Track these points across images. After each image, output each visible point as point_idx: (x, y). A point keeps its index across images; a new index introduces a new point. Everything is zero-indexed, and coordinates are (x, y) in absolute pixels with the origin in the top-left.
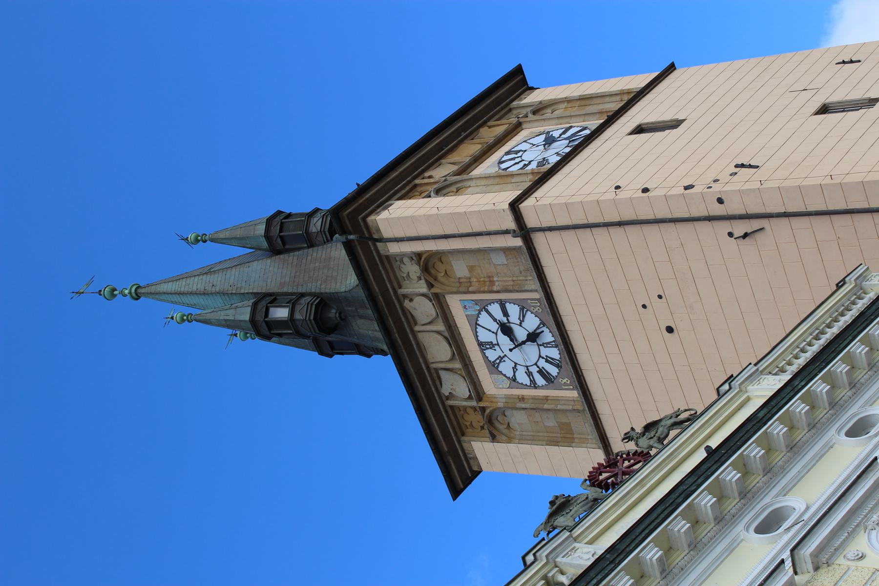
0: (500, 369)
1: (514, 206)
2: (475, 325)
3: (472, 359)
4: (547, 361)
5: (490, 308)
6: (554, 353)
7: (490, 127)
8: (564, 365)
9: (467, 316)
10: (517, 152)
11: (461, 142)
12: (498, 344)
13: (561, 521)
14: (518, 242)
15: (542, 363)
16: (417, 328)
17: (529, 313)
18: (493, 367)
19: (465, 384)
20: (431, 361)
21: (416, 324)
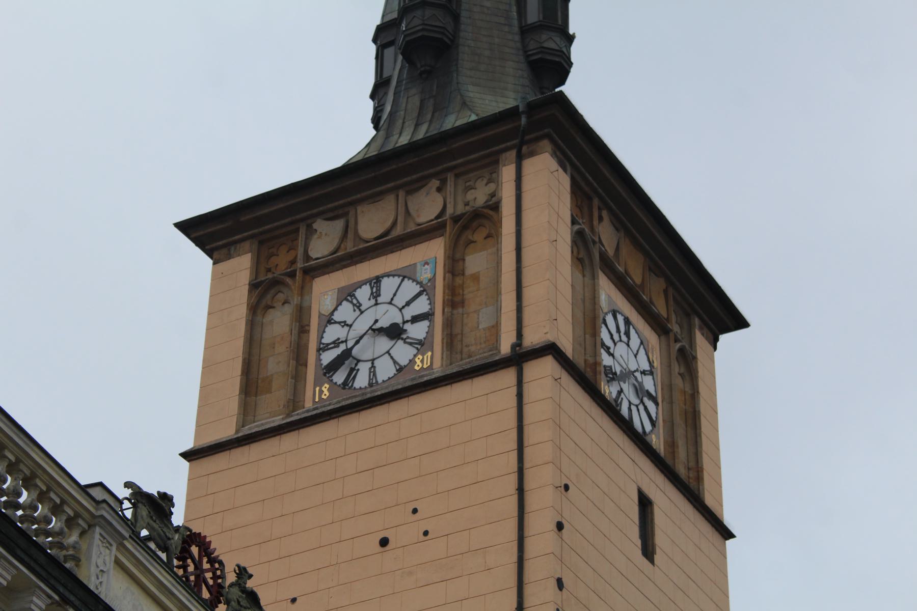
0: (345, 303)
1: (550, 349)
2: (406, 274)
3: (358, 266)
5: (424, 298)
6: (362, 381)
7: (666, 292)
8: (347, 393)
9: (415, 264)
10: (627, 334)
11: (646, 254)
12: (376, 304)
13: (144, 511)
14: (505, 348)
16: (402, 194)
17: (415, 351)
19: (326, 253)
20: (359, 209)
21: (409, 193)
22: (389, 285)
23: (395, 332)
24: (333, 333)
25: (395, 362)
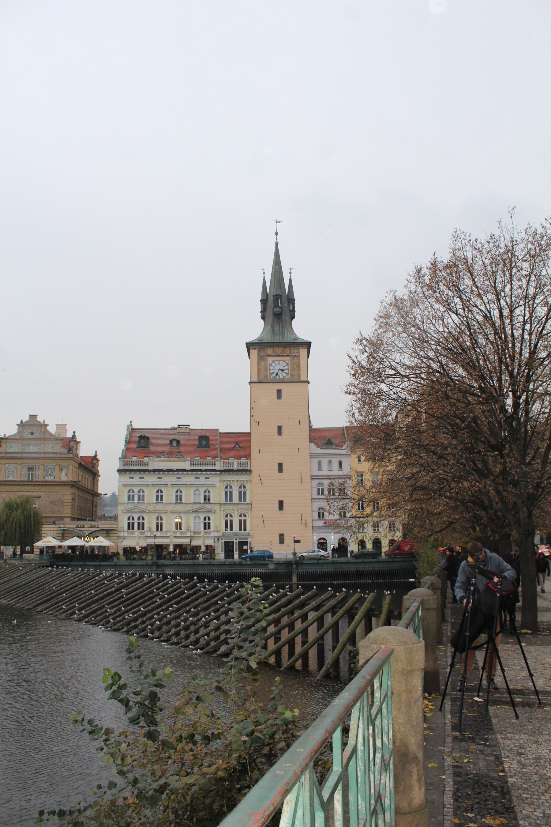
6: (277, 377)
22: (281, 362)
23: (282, 370)
24: (271, 367)
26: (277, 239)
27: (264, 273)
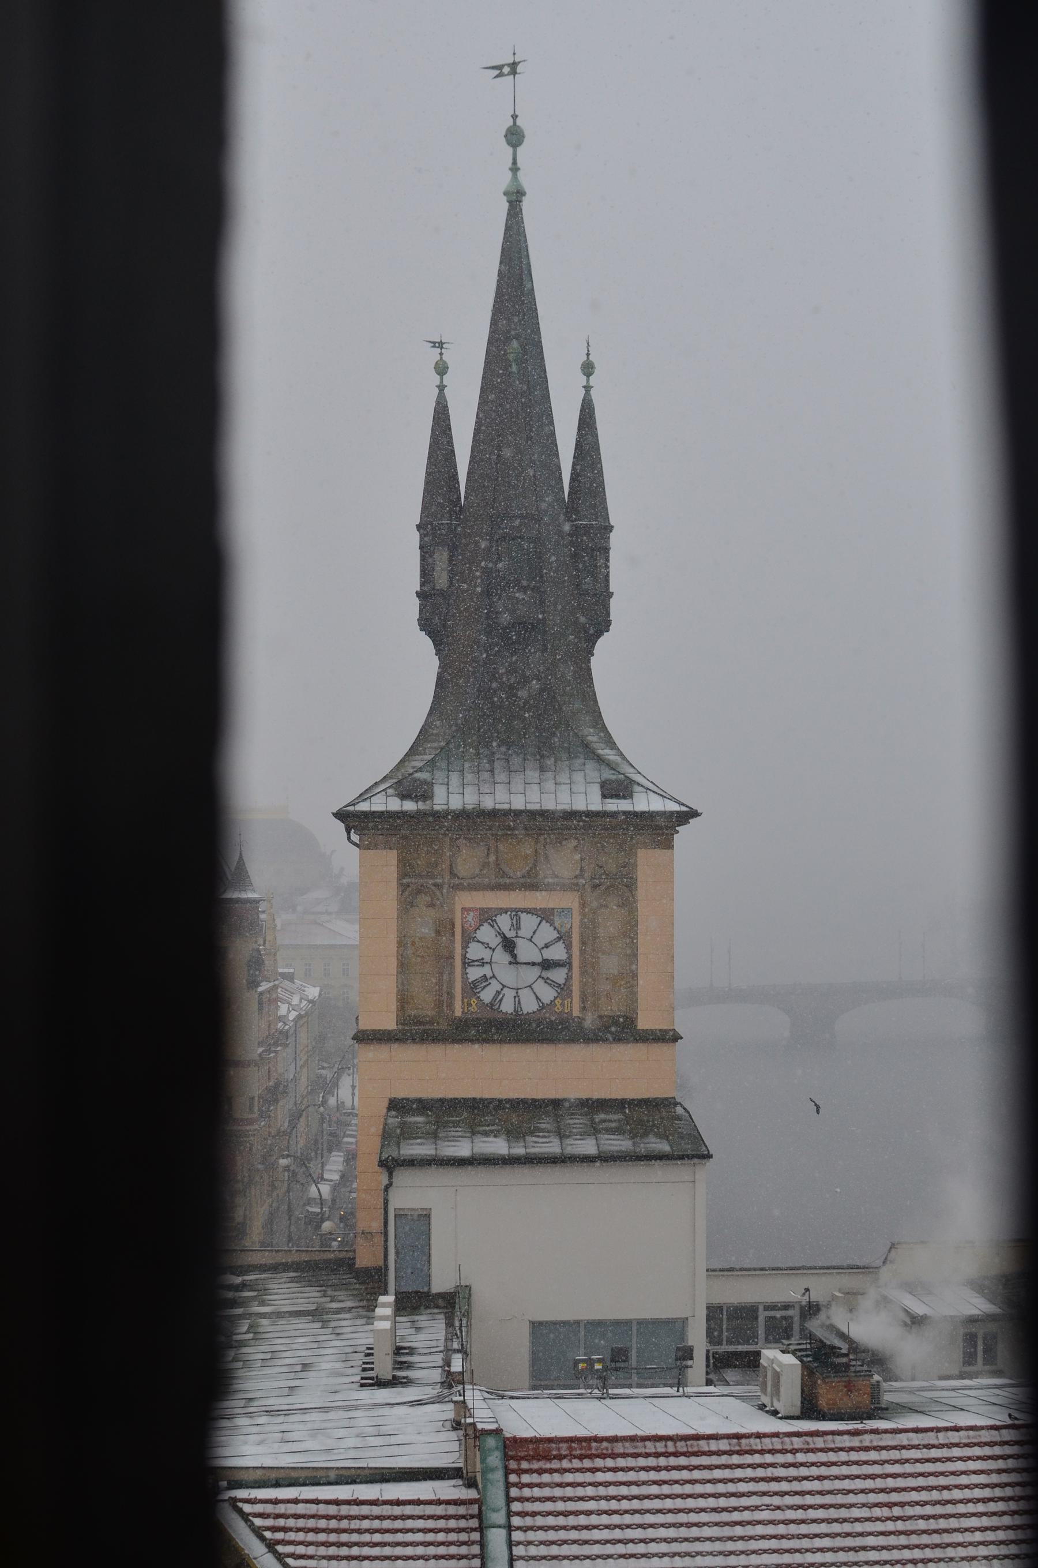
4: (498, 993)
5: (560, 945)
15: (495, 986)
17: (556, 995)
18: (487, 916)
22: (528, 922)
24: (475, 951)
25: (537, 998)
26: (515, 169)
27: (441, 369)
